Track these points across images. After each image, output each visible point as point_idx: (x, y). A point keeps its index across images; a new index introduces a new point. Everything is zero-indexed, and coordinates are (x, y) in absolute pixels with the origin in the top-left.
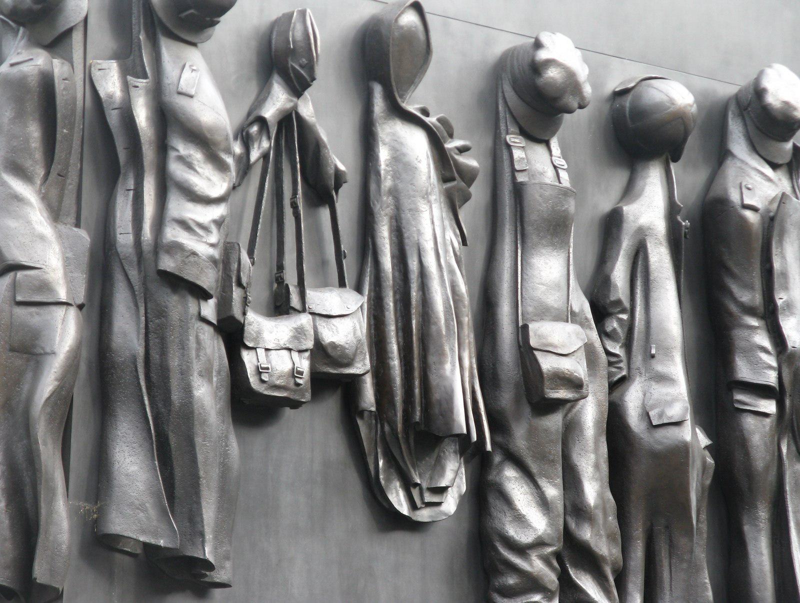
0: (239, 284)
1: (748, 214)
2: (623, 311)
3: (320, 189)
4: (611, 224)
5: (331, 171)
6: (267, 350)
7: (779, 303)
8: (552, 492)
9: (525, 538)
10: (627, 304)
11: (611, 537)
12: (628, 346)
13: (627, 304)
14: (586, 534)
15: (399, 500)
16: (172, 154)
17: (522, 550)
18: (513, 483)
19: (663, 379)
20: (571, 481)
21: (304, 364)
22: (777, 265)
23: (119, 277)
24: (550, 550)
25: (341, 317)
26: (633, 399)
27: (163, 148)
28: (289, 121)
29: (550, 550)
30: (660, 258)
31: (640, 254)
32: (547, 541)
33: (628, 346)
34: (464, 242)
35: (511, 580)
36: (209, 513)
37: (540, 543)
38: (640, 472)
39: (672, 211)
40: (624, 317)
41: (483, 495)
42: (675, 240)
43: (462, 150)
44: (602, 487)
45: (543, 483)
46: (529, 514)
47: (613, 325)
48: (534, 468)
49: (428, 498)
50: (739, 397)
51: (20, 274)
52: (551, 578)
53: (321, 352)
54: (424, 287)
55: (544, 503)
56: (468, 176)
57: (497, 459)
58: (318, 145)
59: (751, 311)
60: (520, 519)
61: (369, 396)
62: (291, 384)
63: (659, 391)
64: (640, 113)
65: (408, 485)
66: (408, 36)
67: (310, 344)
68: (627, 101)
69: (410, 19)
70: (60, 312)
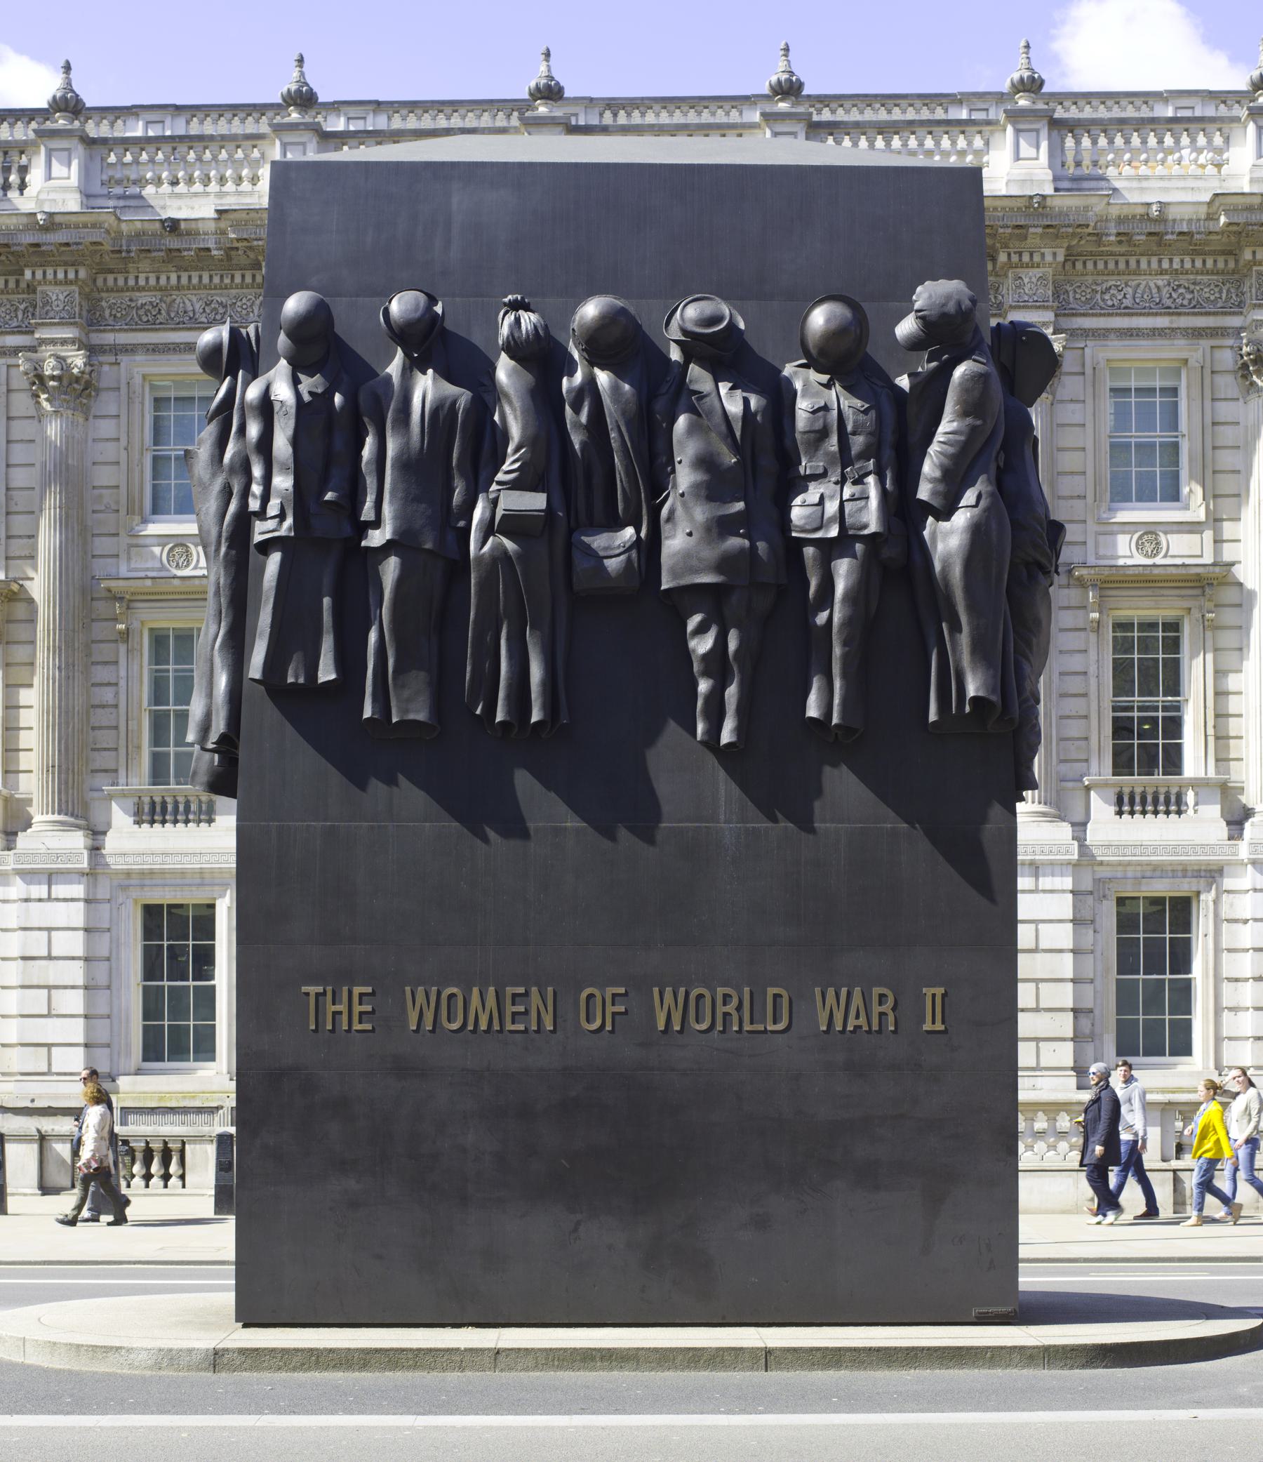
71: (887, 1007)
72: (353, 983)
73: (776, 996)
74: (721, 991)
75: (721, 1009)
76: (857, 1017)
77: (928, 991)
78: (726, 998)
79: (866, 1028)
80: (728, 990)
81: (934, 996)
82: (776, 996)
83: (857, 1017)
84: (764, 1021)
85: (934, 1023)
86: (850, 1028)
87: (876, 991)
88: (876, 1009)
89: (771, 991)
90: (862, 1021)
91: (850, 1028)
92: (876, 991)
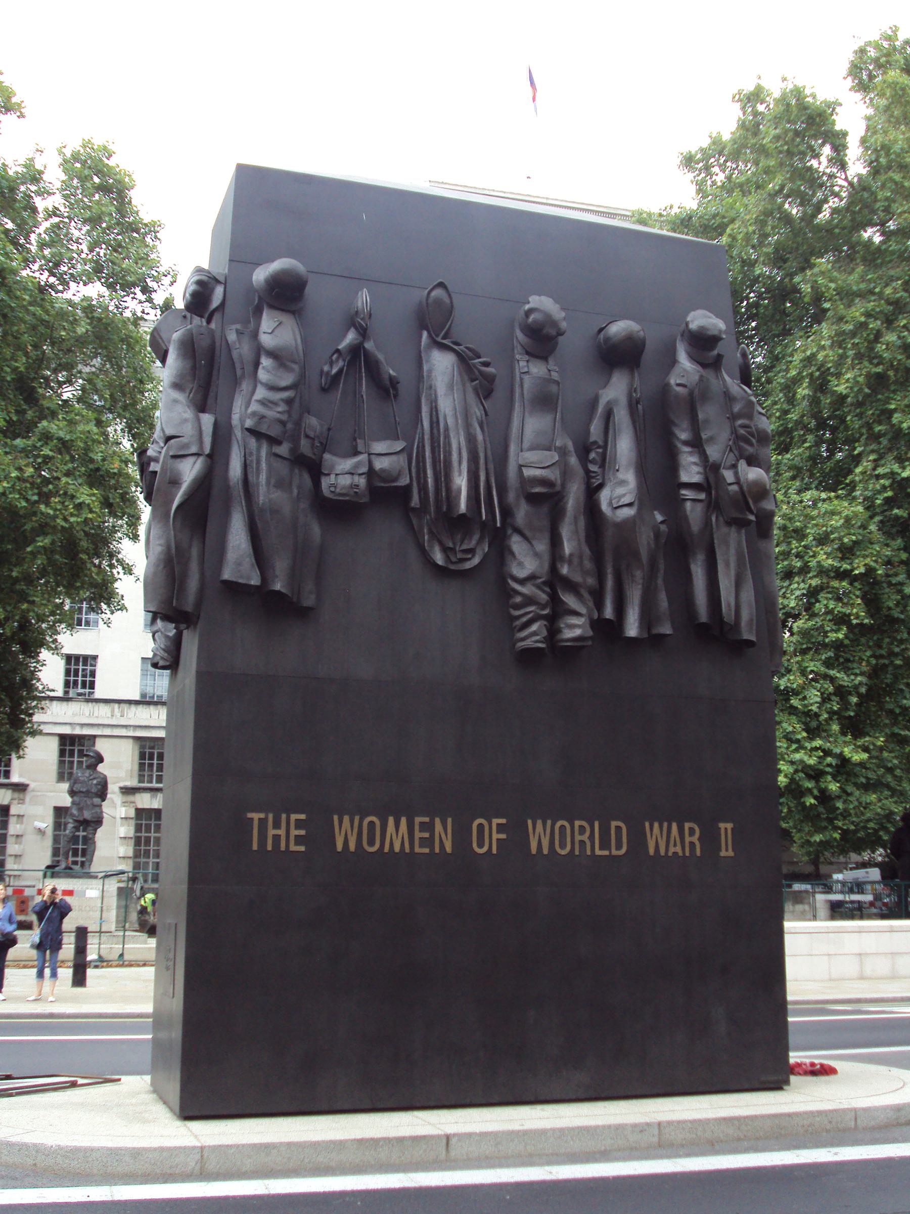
0: (307, 436)
1: (678, 389)
2: (599, 447)
3: (387, 389)
4: (595, 401)
5: (387, 377)
6: (337, 475)
7: (704, 437)
8: (542, 546)
9: (522, 574)
10: (601, 443)
11: (585, 573)
12: (602, 465)
13: (601, 443)
14: (565, 570)
15: (439, 558)
16: (261, 366)
17: (522, 582)
18: (516, 544)
19: (622, 483)
20: (555, 542)
21: (362, 482)
22: (701, 416)
23: (233, 438)
24: (540, 580)
25: (386, 455)
26: (604, 497)
27: (257, 364)
28: (356, 351)
29: (540, 580)
30: (622, 416)
31: (609, 415)
32: (537, 574)
33: (602, 465)
34: (486, 414)
35: (518, 599)
36: (281, 566)
37: (532, 578)
38: (609, 535)
39: (631, 391)
40: (600, 450)
41: (501, 553)
42: (633, 405)
43: (486, 364)
44: (579, 544)
45: (534, 542)
46: (526, 560)
47: (592, 455)
48: (528, 533)
49: (459, 556)
50: (683, 492)
51: (172, 441)
52: (543, 597)
53: (371, 473)
54: (447, 436)
55: (536, 555)
56: (491, 379)
57: (509, 531)
58: (377, 362)
59: (686, 443)
60: (521, 565)
61: (415, 501)
62: (352, 493)
63: (620, 491)
64: (607, 339)
65: (445, 550)
66: (438, 302)
67: (364, 469)
68: (602, 336)
69: (438, 293)
70: (191, 460)
71: (695, 839)
72: (289, 812)
73: (618, 828)
74: (577, 823)
75: (578, 838)
76: (675, 845)
77: (722, 826)
78: (582, 828)
79: (681, 854)
80: (584, 823)
81: (726, 829)
82: (618, 828)
83: (675, 845)
84: (609, 848)
85: (727, 850)
86: (670, 854)
87: (687, 825)
88: (688, 839)
89: (614, 824)
90: (678, 849)
91: (670, 854)
92: (687, 825)
